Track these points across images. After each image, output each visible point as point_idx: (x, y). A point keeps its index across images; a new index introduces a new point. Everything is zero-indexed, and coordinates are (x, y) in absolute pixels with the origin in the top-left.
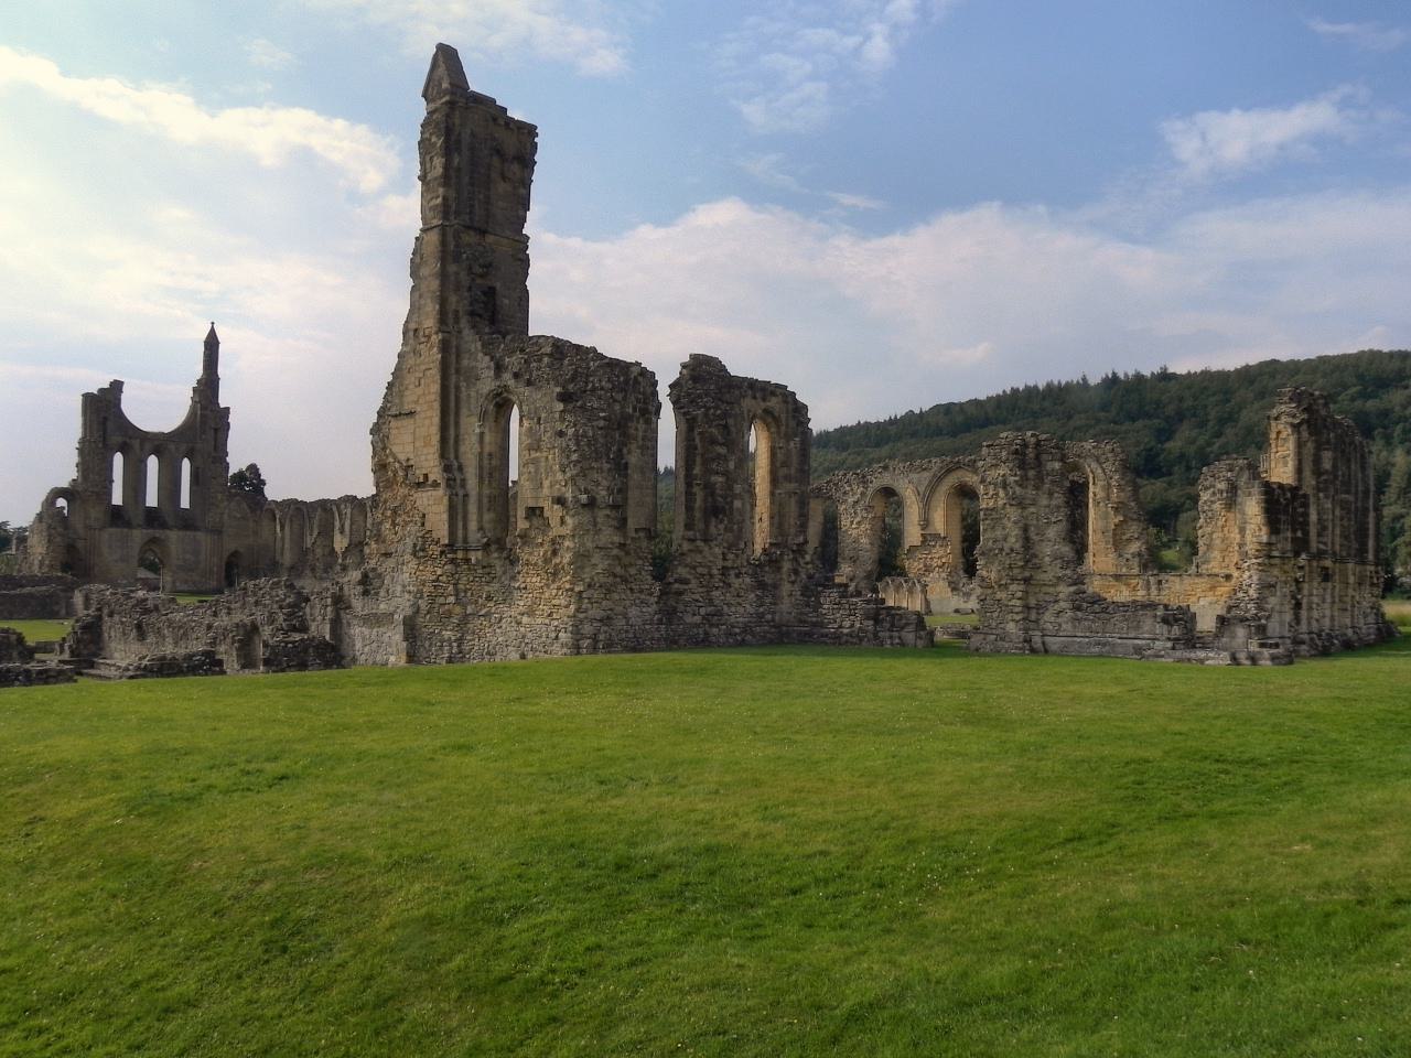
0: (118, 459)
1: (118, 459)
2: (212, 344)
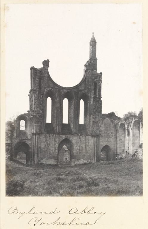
0: (49, 100)
1: (49, 100)
2: (93, 43)
